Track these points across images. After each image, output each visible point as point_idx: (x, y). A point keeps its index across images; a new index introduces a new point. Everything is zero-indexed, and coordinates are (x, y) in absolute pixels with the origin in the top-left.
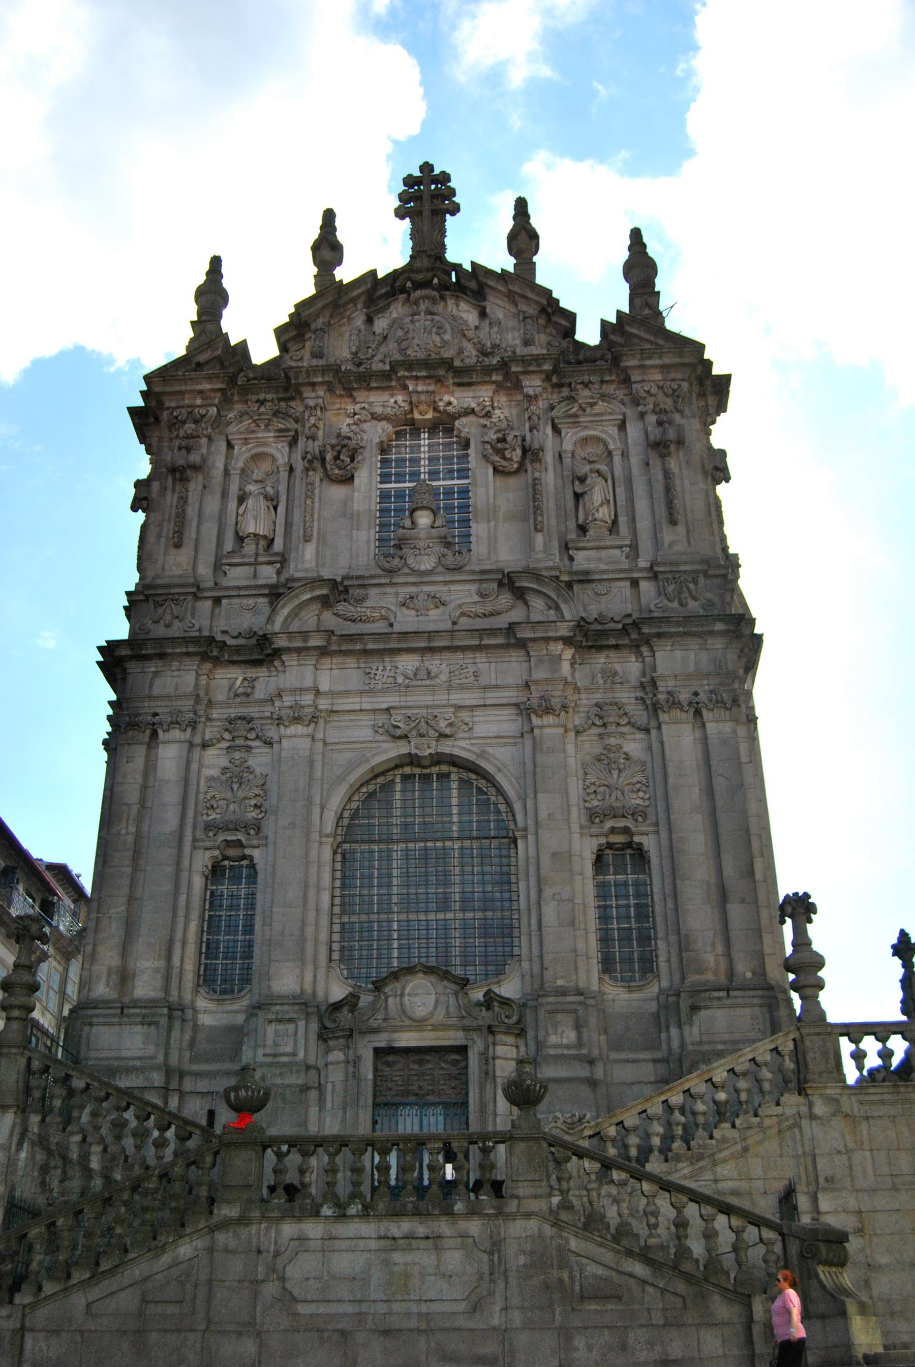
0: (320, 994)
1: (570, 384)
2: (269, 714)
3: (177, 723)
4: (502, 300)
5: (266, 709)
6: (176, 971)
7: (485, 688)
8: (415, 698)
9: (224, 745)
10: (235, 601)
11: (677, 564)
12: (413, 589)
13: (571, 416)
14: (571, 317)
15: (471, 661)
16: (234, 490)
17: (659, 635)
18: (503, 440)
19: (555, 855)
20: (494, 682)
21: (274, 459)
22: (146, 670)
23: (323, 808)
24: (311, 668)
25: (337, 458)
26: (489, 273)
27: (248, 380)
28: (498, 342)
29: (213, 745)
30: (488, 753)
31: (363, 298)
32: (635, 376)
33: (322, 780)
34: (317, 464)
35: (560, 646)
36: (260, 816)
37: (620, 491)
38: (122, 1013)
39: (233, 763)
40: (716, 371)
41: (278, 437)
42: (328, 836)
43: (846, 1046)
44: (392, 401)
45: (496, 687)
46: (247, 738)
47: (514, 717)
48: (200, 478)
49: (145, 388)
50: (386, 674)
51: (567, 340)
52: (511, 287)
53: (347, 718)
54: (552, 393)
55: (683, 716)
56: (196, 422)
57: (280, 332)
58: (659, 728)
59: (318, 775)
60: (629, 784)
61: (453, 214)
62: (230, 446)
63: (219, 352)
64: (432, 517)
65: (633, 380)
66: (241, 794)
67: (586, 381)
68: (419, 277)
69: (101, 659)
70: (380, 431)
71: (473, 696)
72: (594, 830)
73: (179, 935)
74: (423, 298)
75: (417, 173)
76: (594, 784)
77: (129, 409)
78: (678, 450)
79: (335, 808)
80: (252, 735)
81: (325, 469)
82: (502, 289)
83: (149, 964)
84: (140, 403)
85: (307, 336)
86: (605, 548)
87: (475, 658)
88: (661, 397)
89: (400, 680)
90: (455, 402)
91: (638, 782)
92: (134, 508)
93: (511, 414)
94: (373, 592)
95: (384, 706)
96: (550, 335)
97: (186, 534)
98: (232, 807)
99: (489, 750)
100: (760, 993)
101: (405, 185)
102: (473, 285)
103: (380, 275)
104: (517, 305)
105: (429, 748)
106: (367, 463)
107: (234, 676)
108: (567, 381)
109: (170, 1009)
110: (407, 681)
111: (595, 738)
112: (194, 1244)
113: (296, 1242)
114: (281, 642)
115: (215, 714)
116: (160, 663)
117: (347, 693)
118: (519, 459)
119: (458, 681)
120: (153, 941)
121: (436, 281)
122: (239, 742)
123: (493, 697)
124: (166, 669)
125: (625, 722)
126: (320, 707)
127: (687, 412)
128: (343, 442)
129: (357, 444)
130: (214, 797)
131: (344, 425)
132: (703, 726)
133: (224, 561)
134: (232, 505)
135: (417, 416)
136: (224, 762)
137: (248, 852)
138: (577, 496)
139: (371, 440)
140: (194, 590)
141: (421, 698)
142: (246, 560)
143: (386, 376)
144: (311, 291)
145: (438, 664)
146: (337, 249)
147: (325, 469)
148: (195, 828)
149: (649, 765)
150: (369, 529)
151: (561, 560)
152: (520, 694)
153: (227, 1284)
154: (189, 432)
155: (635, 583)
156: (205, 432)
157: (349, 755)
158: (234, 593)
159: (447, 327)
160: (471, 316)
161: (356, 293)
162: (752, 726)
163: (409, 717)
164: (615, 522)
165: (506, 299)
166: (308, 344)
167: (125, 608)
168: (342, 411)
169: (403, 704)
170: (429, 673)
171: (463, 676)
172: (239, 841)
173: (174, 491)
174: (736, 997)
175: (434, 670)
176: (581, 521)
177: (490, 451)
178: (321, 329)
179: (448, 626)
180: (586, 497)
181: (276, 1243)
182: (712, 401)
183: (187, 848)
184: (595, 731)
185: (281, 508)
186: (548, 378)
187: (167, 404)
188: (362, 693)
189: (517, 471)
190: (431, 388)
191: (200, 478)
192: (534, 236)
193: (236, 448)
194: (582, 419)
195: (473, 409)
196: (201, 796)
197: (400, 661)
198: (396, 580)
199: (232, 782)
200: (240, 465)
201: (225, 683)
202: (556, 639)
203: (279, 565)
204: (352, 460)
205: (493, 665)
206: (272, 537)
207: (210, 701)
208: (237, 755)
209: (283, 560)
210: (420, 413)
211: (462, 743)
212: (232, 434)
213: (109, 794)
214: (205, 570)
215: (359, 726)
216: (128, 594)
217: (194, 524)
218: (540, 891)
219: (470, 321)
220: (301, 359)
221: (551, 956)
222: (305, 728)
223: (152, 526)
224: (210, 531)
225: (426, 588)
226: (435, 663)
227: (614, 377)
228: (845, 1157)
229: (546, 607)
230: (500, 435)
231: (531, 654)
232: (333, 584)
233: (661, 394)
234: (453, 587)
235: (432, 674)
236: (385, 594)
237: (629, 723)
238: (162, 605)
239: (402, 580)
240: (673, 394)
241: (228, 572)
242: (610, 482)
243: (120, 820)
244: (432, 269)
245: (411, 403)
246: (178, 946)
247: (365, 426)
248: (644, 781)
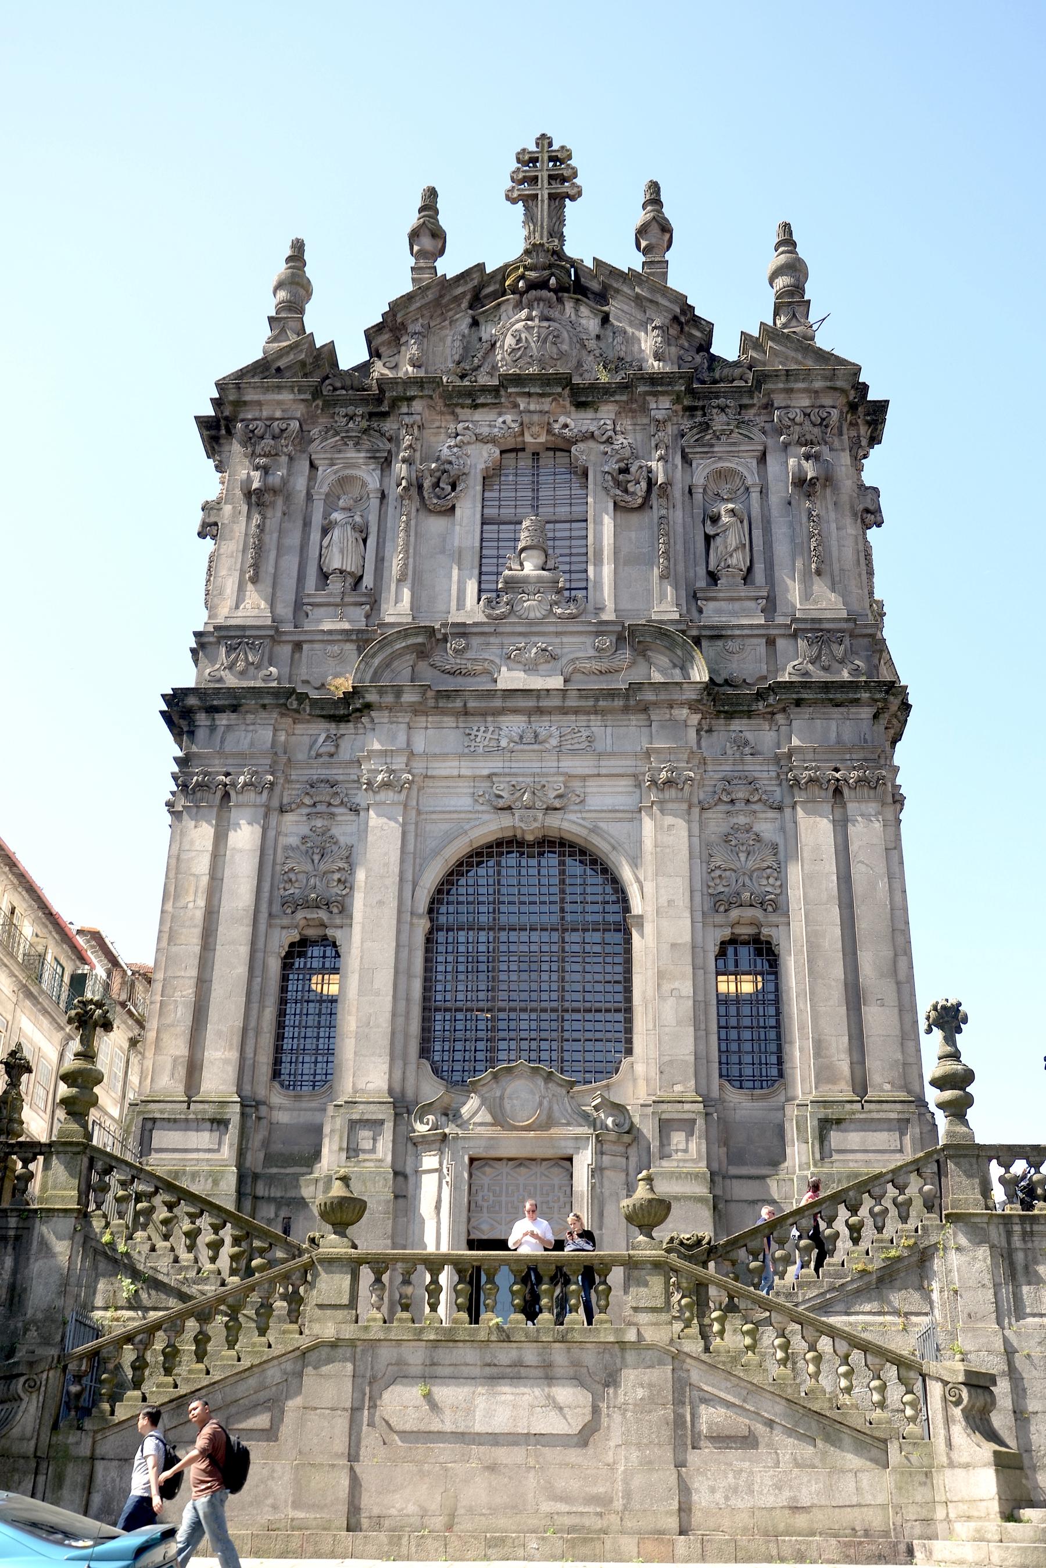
0: (410, 1093)
1: (703, 408)
2: (356, 778)
3: (252, 785)
4: (627, 304)
5: (352, 771)
6: (249, 1062)
7: (600, 755)
8: (521, 765)
9: (305, 811)
10: (317, 646)
11: (820, 620)
12: (520, 639)
13: (703, 446)
14: (707, 329)
15: (584, 724)
16: (317, 520)
17: (798, 703)
18: (625, 471)
19: (673, 946)
20: (609, 749)
21: (364, 484)
23: (415, 884)
24: (404, 726)
25: (437, 485)
26: (614, 272)
27: (335, 389)
28: (622, 354)
29: (292, 811)
30: (601, 829)
31: (468, 297)
32: (779, 400)
33: (414, 854)
34: (414, 491)
35: (685, 711)
36: (344, 892)
37: (757, 533)
38: (189, 1108)
39: (314, 832)
40: (871, 397)
41: (370, 458)
42: (420, 916)
43: (995, 1170)
44: (501, 420)
45: (612, 754)
46: (330, 804)
47: (631, 789)
48: (280, 502)
49: (217, 396)
50: (489, 735)
51: (701, 354)
52: (637, 290)
53: (443, 784)
54: (683, 416)
55: (823, 793)
56: (274, 438)
57: (370, 335)
58: (794, 808)
59: (411, 848)
60: (758, 869)
61: (573, 199)
62: (313, 466)
63: (303, 356)
64: (543, 558)
65: (776, 405)
66: (323, 867)
67: (723, 405)
68: (532, 275)
69: (165, 708)
70: (485, 455)
71: (586, 764)
72: (719, 919)
73: (253, 1024)
74: (539, 300)
75: (533, 148)
76: (719, 867)
77: (196, 417)
78: (825, 486)
79: (428, 886)
80: (337, 802)
81: (422, 498)
82: (629, 292)
83: (218, 1054)
84: (209, 411)
85: (403, 340)
86: (739, 599)
87: (589, 721)
88: (807, 426)
89: (504, 743)
90: (572, 424)
91: (768, 867)
92: (202, 535)
93: (636, 440)
94: (475, 641)
95: (486, 772)
96: (682, 347)
97: (262, 569)
98: (312, 881)
99: (602, 825)
100: (898, 1106)
101: (518, 161)
102: (595, 286)
103: (488, 271)
104: (645, 312)
105: (535, 820)
106: (471, 492)
107: (316, 732)
108: (701, 403)
109: (243, 1106)
110: (512, 745)
111: (721, 816)
112: (283, 1366)
113: (395, 1368)
114: (371, 697)
115: (294, 775)
116: (233, 716)
117: (444, 756)
118: (643, 494)
119: (569, 747)
120: (225, 1029)
121: (553, 281)
122: (321, 808)
123: (610, 765)
124: (240, 722)
125: (756, 799)
126: (414, 771)
127: (837, 444)
128: (442, 467)
129: (459, 469)
130: (292, 869)
131: (445, 448)
132: (844, 806)
133: (305, 601)
134: (315, 535)
135: (528, 438)
136: (305, 830)
137: (330, 932)
138: (708, 539)
139: (475, 465)
140: (272, 633)
141: (527, 765)
142: (332, 600)
143: (495, 391)
144: (407, 287)
145: (549, 728)
146: (438, 235)
147: (422, 498)
148: (270, 903)
149: (781, 848)
150: (472, 568)
151: (688, 611)
152: (639, 763)
153: (318, 1411)
154: (267, 449)
155: (771, 642)
156: (285, 450)
157: (445, 826)
158: (320, 637)
159: (565, 335)
160: (592, 321)
161: (460, 290)
162: (898, 806)
163: (513, 786)
164: (750, 569)
165: (633, 304)
166: (403, 348)
167: (192, 650)
168: (442, 430)
169: (507, 770)
170: (536, 736)
171: (576, 741)
172: (320, 919)
173: (249, 517)
174: (870, 1112)
175: (543, 733)
176: (711, 568)
177: (611, 483)
178: (419, 333)
179: (556, 682)
180: (718, 539)
181: (372, 1368)
182: (864, 431)
183: (262, 927)
184: (722, 808)
185: (371, 542)
186: (678, 400)
187: (241, 416)
188: (461, 756)
189: (641, 507)
190: (546, 408)
191: (280, 502)
192: (666, 228)
193: (320, 468)
194: (716, 449)
195: (593, 433)
196: (278, 868)
197: (504, 722)
198: (500, 630)
199: (313, 853)
200: (325, 489)
201: (306, 740)
202: (682, 704)
203: (368, 607)
204: (454, 488)
205: (609, 730)
206: (360, 574)
207: (289, 760)
208: (319, 823)
209: (374, 601)
211: (573, 817)
212: (316, 453)
213: (173, 861)
214: (285, 611)
216: (197, 634)
217: (273, 555)
219: (591, 328)
220: (396, 367)
221: (667, 1058)
222: (396, 795)
223: (223, 558)
224: (291, 563)
225: (535, 639)
226: (544, 726)
227: (755, 401)
228: (992, 1291)
229: (671, 665)
230: (622, 465)
231: (652, 718)
232: (431, 631)
233: (807, 423)
234: (565, 640)
235: (541, 738)
236: (488, 644)
237: (760, 800)
238: (235, 649)
239: (508, 629)
240: (821, 424)
241: (310, 613)
242: (746, 523)
243: (187, 892)
244: (550, 266)
245: (522, 424)
246: (251, 1034)
247: (470, 450)
248: (776, 866)
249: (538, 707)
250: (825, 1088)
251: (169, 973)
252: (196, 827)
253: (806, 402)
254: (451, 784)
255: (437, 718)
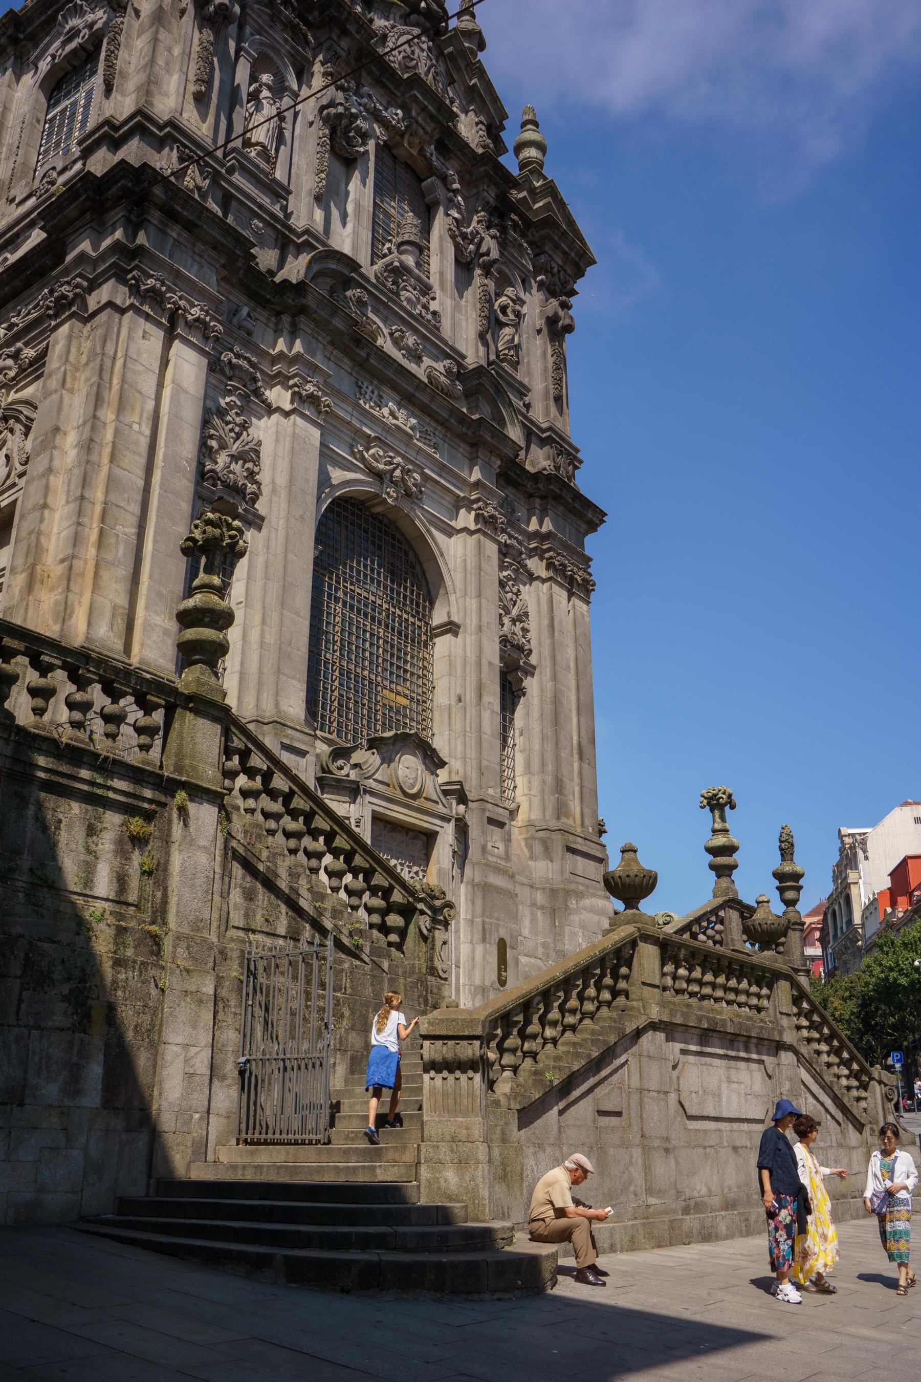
22: (169, 231)
53: (333, 422)
87: (436, 429)
88: (557, 278)
114: (310, 302)
116: (186, 235)
120: (165, 592)
210: (409, 144)
215: (339, 437)
218: (480, 696)
249: (414, 396)
250: (564, 820)
251: (112, 498)
252: (143, 337)
253: (560, 263)
254: (339, 426)
255: (340, 355)
